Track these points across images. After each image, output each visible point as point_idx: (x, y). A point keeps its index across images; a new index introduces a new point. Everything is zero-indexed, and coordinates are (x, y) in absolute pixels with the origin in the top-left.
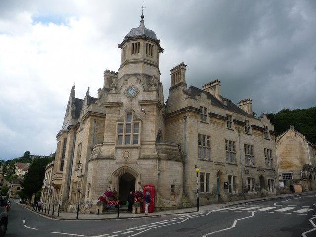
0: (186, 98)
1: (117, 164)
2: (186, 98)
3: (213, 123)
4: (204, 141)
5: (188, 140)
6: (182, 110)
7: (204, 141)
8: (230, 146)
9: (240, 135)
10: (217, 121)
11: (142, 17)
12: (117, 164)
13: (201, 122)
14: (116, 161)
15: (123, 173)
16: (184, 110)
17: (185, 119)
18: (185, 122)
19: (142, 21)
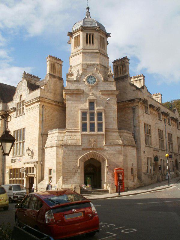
0: (134, 91)
1: (83, 149)
2: (134, 91)
3: (151, 113)
4: (147, 128)
5: (138, 129)
6: (130, 101)
7: (147, 128)
8: (160, 132)
9: (165, 125)
10: (153, 112)
11: (88, 9)
12: (83, 149)
13: (145, 113)
14: (83, 147)
15: (89, 158)
16: (132, 101)
17: (134, 109)
18: (134, 112)
19: (89, 12)
